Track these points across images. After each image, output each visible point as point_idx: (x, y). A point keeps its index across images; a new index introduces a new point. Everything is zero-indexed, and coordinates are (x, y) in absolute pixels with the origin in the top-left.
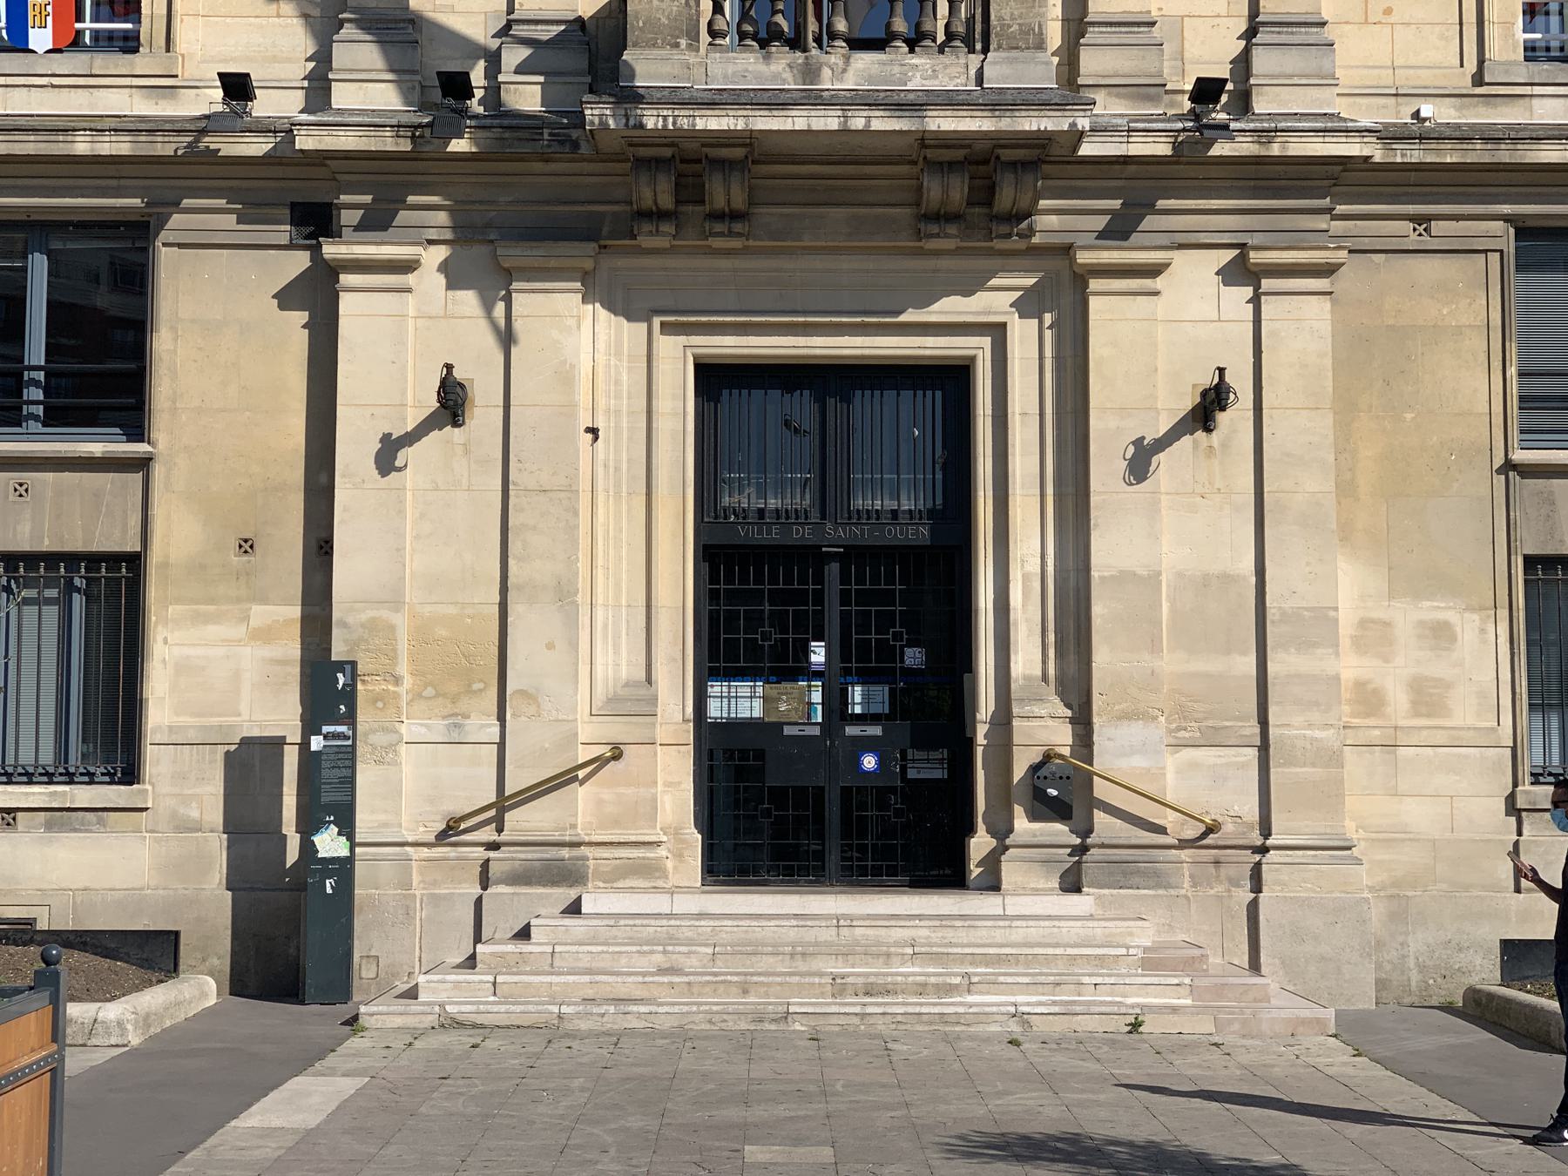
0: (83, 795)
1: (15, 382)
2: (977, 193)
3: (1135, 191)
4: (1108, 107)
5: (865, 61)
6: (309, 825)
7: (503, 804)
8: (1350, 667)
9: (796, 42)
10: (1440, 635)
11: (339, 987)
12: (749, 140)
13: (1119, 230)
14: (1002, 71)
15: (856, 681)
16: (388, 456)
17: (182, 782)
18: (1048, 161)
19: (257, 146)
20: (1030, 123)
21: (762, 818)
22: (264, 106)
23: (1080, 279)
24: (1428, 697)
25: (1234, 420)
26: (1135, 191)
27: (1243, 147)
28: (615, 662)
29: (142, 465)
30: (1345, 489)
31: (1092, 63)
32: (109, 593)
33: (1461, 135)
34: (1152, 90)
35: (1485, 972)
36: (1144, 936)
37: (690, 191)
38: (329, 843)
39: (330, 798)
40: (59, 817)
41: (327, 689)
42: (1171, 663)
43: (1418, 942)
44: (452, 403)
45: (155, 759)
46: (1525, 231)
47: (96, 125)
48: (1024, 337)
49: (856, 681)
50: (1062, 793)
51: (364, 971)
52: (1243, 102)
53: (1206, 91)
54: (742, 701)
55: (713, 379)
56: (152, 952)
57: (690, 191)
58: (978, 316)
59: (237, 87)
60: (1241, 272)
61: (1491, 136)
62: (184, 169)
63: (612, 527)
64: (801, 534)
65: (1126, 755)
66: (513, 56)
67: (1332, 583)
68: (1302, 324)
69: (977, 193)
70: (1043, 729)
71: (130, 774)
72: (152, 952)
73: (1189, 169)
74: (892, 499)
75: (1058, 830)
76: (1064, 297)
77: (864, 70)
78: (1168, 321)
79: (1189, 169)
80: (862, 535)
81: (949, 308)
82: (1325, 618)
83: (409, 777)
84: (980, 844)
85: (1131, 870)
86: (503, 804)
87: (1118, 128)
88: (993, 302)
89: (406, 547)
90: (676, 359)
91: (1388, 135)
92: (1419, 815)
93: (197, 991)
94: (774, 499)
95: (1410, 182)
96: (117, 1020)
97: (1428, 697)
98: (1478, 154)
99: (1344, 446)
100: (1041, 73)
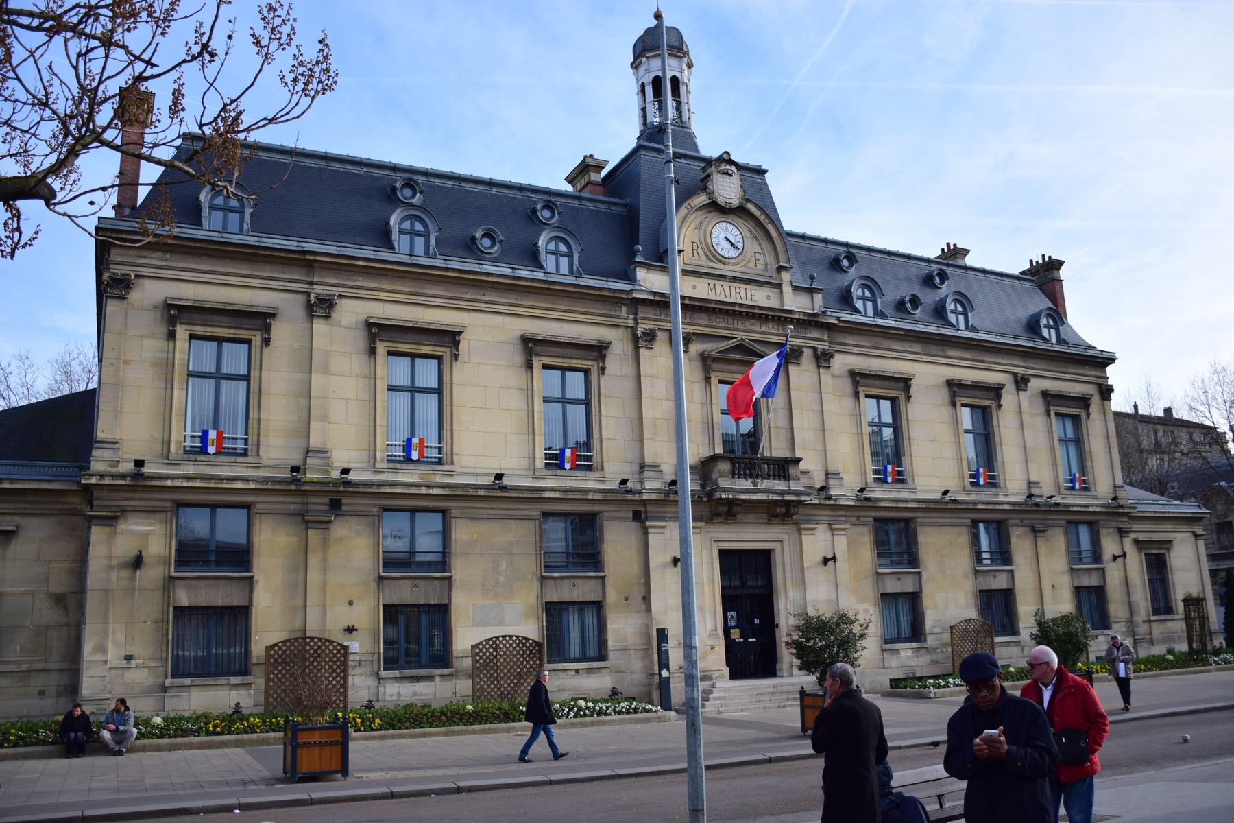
6: (660, 670)
9: (751, 477)
29: (603, 578)
38: (665, 673)
40: (589, 671)
45: (611, 655)
55: (723, 553)
64: (738, 592)
74: (754, 582)
78: (817, 542)
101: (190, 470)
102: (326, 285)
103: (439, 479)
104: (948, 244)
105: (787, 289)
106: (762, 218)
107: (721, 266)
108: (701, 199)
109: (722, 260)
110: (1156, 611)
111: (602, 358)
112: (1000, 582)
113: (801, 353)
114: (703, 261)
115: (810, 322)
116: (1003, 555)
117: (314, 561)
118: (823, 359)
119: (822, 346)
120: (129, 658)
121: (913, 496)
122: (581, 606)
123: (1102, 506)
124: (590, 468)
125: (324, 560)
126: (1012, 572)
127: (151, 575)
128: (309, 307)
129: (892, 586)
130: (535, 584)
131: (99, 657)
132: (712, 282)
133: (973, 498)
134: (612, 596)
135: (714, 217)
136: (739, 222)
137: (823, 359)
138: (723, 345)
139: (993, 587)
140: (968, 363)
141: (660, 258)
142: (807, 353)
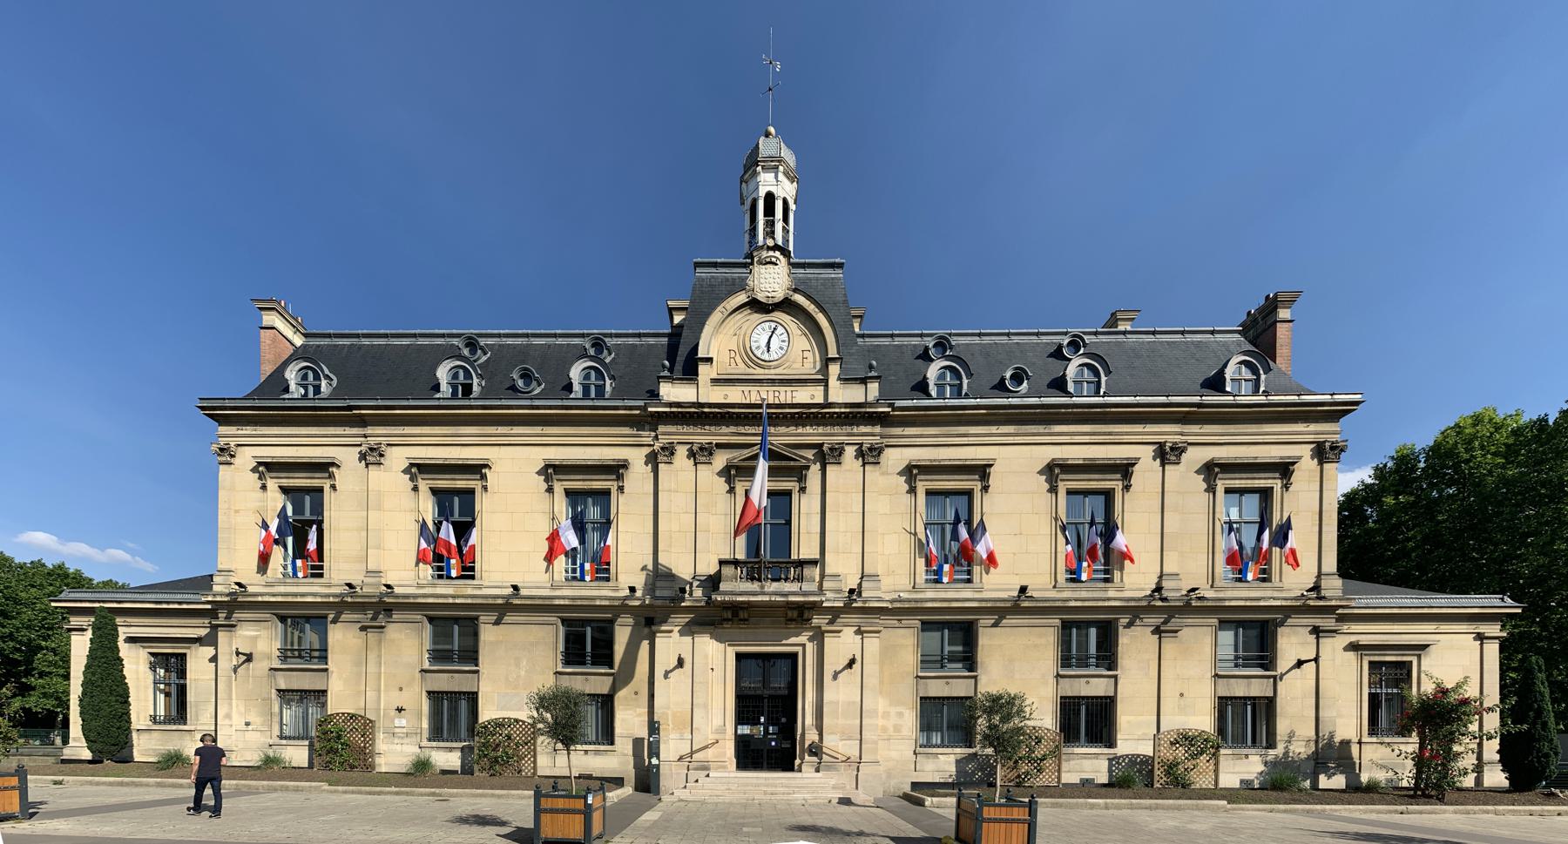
0: (602, 748)
1: (584, 656)
2: (799, 615)
3: (835, 613)
4: (829, 595)
5: (775, 584)
7: (692, 753)
8: (881, 722)
10: (900, 715)
11: (658, 793)
12: (749, 602)
13: (831, 622)
14: (806, 587)
15: (771, 725)
16: (666, 675)
17: (623, 745)
18: (815, 607)
19: (637, 603)
20: (812, 599)
21: (750, 756)
22: (639, 594)
23: (823, 633)
24: (897, 728)
25: (857, 666)
26: (835, 613)
27: (859, 604)
28: (718, 721)
30: (881, 682)
31: (826, 585)
32: (606, 704)
33: (909, 601)
34: (839, 591)
35: (907, 789)
36: (833, 782)
37: (735, 614)
38: (654, 761)
39: (654, 751)
40: (597, 752)
41: (654, 727)
42: (841, 721)
43: (893, 782)
44: (681, 663)
45: (617, 740)
46: (923, 623)
47: (601, 598)
48: (810, 647)
49: (771, 725)
50: (816, 750)
51: (662, 788)
52: (860, 594)
53: (852, 591)
54: (745, 730)
55: (740, 657)
56: (618, 782)
57: (735, 614)
58: (799, 642)
59: (632, 589)
60: (859, 632)
61: (916, 601)
62: (621, 608)
63: (717, 690)
65: (830, 742)
66: (696, 584)
67: (877, 703)
68: (872, 644)
69: (799, 615)
70: (812, 736)
71: (612, 743)
72: (618, 782)
73: (848, 608)
75: (815, 759)
76: (819, 637)
77: (774, 587)
78: (844, 642)
79: (848, 608)
80: (772, 692)
81: (793, 640)
82: (876, 712)
83: (672, 747)
84: (797, 762)
85: (829, 768)
86: (692, 753)
87: (832, 600)
88: (803, 639)
89: (671, 695)
90: (731, 652)
91: (892, 601)
92: (894, 754)
93: (628, 790)
94: (752, 684)
95: (897, 612)
96: (614, 795)
97: (897, 728)
98: (913, 605)
99: (881, 671)
100: (814, 587)
101: (282, 589)
103: (470, 591)
105: (833, 382)
106: (811, 308)
108: (742, 298)
111: (620, 478)
112: (1097, 687)
113: (841, 452)
114: (742, 365)
115: (855, 416)
117: (372, 657)
118: (870, 455)
119: (868, 441)
120: (247, 724)
121: (977, 596)
123: (1296, 599)
124: (608, 579)
125: (380, 656)
126: (1115, 677)
127: (260, 667)
128: (363, 457)
131: (227, 722)
132: (746, 389)
133: (1066, 595)
135: (757, 317)
138: (746, 453)
141: (689, 372)
142: (850, 452)
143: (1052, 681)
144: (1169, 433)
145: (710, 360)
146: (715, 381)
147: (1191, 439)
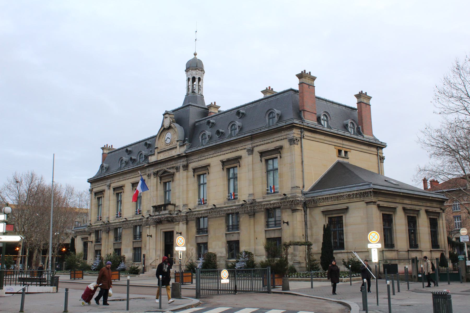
102: (108, 182)
104: (269, 87)
107: (167, 147)
109: (167, 144)
110: (411, 246)
115: (179, 157)
116: (236, 227)
118: (186, 167)
121: (207, 208)
122: (138, 248)
129: (200, 241)
130: (132, 243)
134: (143, 246)
136: (171, 131)
137: (186, 167)
139: (232, 240)
140: (229, 151)
143: (225, 236)
144: (249, 145)
145: (156, 148)
146: (159, 153)
147: (254, 145)
